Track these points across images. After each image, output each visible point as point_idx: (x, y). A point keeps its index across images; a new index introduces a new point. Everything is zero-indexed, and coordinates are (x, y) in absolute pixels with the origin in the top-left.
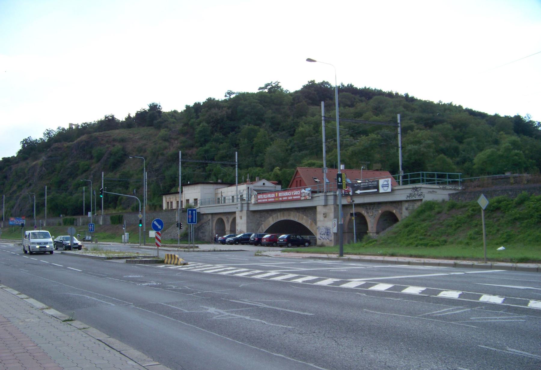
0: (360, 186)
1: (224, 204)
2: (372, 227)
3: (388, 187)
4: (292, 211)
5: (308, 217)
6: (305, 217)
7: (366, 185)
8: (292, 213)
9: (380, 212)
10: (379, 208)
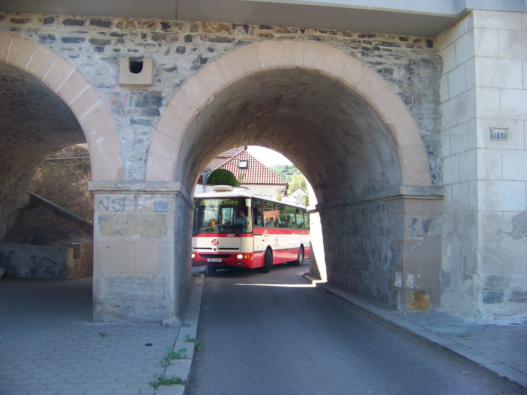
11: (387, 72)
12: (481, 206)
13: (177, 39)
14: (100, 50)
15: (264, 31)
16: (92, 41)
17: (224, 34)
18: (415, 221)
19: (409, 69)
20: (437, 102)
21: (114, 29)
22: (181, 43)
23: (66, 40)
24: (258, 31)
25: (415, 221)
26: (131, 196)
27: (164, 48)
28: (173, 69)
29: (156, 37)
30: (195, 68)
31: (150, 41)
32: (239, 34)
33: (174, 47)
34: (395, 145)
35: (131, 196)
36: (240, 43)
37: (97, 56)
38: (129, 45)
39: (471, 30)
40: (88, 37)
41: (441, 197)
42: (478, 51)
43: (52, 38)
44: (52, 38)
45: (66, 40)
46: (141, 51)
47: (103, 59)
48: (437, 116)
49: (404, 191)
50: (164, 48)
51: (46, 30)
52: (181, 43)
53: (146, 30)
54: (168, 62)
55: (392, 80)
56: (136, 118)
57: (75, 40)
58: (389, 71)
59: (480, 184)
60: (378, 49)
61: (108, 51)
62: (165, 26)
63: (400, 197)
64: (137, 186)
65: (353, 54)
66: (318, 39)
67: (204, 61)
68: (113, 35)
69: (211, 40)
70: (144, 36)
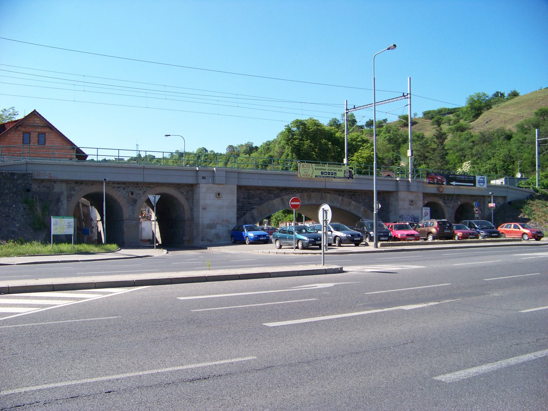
0: (456, 178)
1: (262, 171)
2: (450, 217)
3: (484, 183)
4: (329, 193)
5: (359, 202)
6: (353, 202)
7: (462, 178)
8: (329, 195)
9: (459, 203)
10: (458, 200)
11: (182, 193)
12: (200, 223)
13: (139, 187)
16: (123, 188)
17: (149, 186)
18: (188, 225)
19: (187, 192)
20: (193, 199)
23: (117, 188)
24: (156, 185)
25: (188, 225)
26: (131, 221)
27: (137, 189)
28: (139, 194)
29: (135, 187)
30: (143, 194)
31: (134, 188)
32: (152, 186)
33: (139, 189)
36: (152, 188)
37: (124, 191)
39: (200, 187)
40: (122, 187)
41: (193, 220)
44: (115, 187)
45: (117, 188)
47: (125, 192)
48: (193, 202)
49: (186, 219)
50: (137, 189)
51: (113, 186)
52: (140, 188)
54: (138, 192)
55: (184, 195)
56: (132, 204)
57: (119, 188)
58: (183, 193)
59: (200, 218)
61: (126, 190)
62: (137, 184)
64: (132, 219)
65: (175, 189)
66: (168, 186)
67: (145, 192)
68: (127, 186)
70: (133, 186)
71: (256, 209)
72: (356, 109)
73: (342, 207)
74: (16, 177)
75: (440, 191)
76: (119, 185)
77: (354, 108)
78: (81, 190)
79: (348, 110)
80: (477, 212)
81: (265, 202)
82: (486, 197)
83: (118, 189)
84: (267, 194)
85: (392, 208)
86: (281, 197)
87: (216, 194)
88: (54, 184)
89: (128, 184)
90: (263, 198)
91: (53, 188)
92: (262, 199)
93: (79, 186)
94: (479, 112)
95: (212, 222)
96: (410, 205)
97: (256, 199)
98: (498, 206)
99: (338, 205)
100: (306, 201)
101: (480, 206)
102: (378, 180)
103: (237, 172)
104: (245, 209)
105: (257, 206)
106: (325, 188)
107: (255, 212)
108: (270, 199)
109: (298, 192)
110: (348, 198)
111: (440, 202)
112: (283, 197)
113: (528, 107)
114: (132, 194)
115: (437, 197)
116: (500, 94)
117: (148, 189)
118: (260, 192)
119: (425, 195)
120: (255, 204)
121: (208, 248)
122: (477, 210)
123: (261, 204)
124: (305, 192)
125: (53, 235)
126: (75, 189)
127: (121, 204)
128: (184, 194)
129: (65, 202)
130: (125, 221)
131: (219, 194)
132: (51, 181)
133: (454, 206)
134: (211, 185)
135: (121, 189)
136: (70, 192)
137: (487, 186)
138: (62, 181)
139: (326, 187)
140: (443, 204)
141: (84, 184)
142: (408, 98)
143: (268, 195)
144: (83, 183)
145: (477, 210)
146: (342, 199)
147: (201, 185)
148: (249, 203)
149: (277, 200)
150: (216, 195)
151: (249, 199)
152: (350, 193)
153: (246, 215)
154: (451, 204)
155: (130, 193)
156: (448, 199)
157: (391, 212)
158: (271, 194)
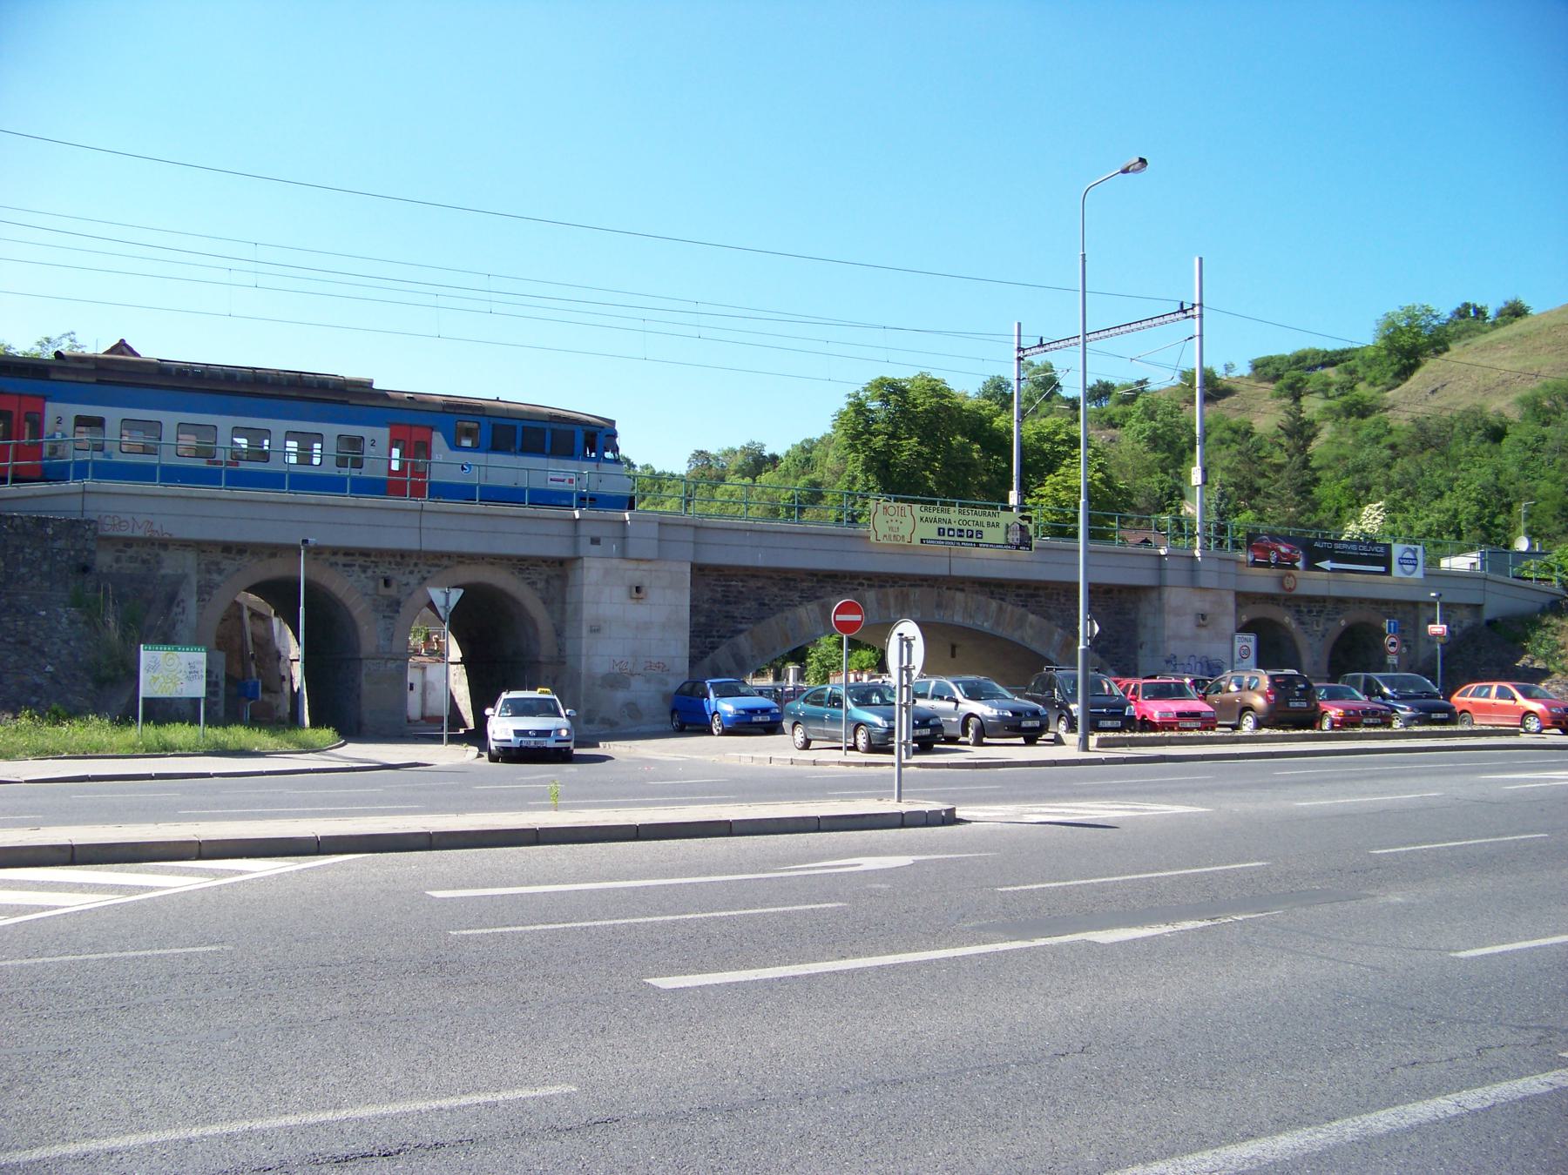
0: (1333, 549)
2: (1315, 663)
3: (1416, 565)
4: (962, 590)
5: (1049, 618)
6: (1031, 617)
7: (1351, 550)
8: (959, 596)
9: (1343, 623)
10: (1338, 613)
11: (532, 584)
12: (584, 670)
13: (408, 565)
14: (364, 572)
15: (460, 559)
16: (360, 566)
17: (436, 561)
19: (547, 582)
20: (564, 602)
21: (373, 559)
22: (411, 568)
23: (345, 565)
25: (547, 677)
26: (383, 662)
27: (401, 572)
28: (407, 584)
29: (397, 564)
30: (420, 584)
32: (445, 562)
34: (536, 629)
35: (383, 662)
36: (446, 567)
37: (363, 576)
38: (382, 569)
39: (582, 568)
41: (564, 663)
42: (586, 582)
43: (337, 564)
44: (337, 564)
45: (345, 565)
46: (389, 573)
47: (367, 578)
48: (563, 611)
49: (541, 659)
51: (333, 559)
52: (411, 568)
53: (391, 559)
56: (386, 614)
60: (528, 569)
61: (370, 573)
63: (539, 662)
64: (387, 656)
65: (513, 573)
66: (492, 564)
67: (424, 579)
68: (372, 562)
69: (430, 566)
70: (390, 563)
71: (746, 633)
72: (1047, 348)
73: (999, 632)
74: (50, 531)
75: (1287, 586)
76: (350, 558)
77: (1041, 345)
78: (238, 570)
79: (1024, 350)
80: (1392, 649)
81: (774, 614)
82: (1421, 606)
83: (347, 569)
84: (781, 589)
85: (1144, 635)
86: (822, 601)
87: (631, 587)
88: (163, 553)
89: (376, 556)
90: (766, 602)
91: (158, 562)
92: (764, 605)
93: (235, 560)
94: (1412, 361)
95: (617, 669)
96: (1199, 626)
97: (748, 605)
98: (1457, 633)
99: (985, 624)
100: (892, 611)
101: (1403, 631)
102: (1090, 552)
103: (691, 526)
104: (715, 633)
105: (751, 626)
106: (950, 576)
107: (743, 641)
108: (789, 605)
109: (870, 586)
110: (1018, 605)
111: (1287, 619)
112: (826, 599)
113: (1553, 348)
114: (387, 583)
115: (1278, 605)
116: (1474, 311)
117: (434, 569)
118: (760, 585)
119: (1243, 598)
120: (743, 618)
121: (601, 744)
122: (1393, 644)
123: (763, 618)
124: (891, 586)
125: (144, 699)
126: (222, 567)
127: (355, 613)
128: (539, 586)
129: (192, 603)
130: (364, 662)
131: (638, 589)
132: (153, 544)
133: (1327, 630)
134: (615, 562)
135: (356, 568)
136: (208, 576)
137: (1425, 575)
138: (185, 544)
139: (953, 573)
140: (1294, 626)
141: (248, 554)
142: (1193, 316)
143: (783, 593)
144: (246, 551)
145: (1393, 644)
146: (1000, 608)
147: (587, 562)
148: (726, 617)
149: (809, 607)
150: (631, 591)
151: (728, 603)
152: (1021, 592)
153: (716, 651)
154: (1318, 626)
155: (382, 582)
156: (1310, 612)
157: (1141, 647)
158: (791, 590)
